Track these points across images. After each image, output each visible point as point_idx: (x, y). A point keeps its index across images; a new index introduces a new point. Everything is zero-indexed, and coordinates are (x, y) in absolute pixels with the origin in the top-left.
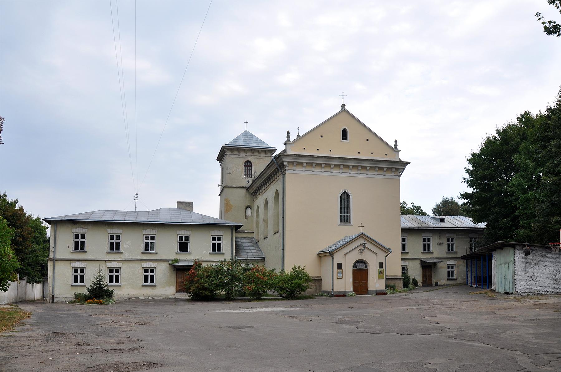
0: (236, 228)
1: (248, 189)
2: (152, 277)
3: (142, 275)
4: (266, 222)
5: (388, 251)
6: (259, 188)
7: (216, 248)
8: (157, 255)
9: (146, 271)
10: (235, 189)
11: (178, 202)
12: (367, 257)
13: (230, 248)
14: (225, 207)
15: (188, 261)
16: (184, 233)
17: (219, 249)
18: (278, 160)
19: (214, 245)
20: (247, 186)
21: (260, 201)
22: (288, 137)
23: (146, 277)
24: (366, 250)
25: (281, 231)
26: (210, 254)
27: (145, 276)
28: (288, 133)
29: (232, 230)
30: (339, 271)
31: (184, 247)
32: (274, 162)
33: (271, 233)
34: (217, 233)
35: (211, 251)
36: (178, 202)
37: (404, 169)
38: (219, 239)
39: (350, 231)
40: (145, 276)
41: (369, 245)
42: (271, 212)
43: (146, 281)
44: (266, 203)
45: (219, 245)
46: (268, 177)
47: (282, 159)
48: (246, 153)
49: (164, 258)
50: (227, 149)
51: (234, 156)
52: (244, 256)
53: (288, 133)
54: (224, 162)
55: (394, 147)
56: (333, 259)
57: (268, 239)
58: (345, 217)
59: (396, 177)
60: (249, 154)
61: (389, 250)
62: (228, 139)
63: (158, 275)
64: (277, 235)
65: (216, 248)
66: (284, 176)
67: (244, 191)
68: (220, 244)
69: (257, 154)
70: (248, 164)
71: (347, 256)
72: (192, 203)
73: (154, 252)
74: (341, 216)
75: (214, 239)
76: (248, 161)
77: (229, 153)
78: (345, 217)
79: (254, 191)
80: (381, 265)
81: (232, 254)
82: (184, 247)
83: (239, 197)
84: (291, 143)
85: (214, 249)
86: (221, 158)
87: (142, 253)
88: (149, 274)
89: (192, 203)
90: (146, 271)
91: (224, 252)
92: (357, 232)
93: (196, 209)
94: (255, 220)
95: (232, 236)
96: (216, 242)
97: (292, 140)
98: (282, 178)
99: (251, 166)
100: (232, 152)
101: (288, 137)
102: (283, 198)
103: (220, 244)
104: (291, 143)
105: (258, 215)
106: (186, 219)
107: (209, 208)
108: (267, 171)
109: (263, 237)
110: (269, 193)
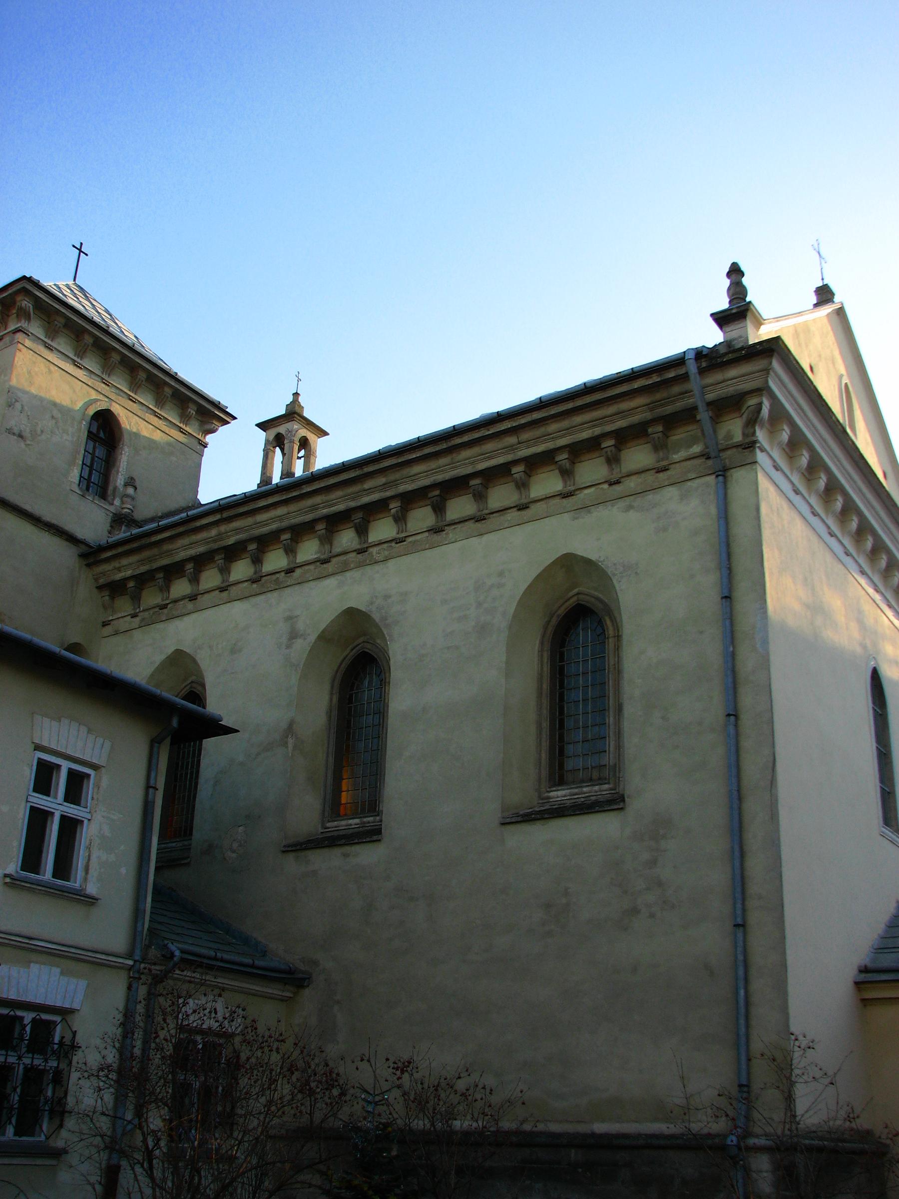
13: (127, 872)
18: (711, 379)
22: (737, 291)
26: (13, 882)
28: (735, 272)
29: (154, 743)
35: (13, 867)
47: (767, 371)
51: (52, 357)
53: (735, 272)
57: (367, 856)
60: (120, 382)
75: (44, 778)
77: (36, 328)
91: (92, 889)
100: (52, 332)
101: (737, 291)
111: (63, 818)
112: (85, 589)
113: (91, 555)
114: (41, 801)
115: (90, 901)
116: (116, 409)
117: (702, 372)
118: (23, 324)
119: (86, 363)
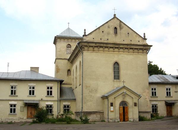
0: (61, 82)
1: (69, 60)
2: (14, 109)
3: (9, 108)
4: (76, 78)
5: (139, 96)
6: (73, 59)
7: (49, 93)
8: (18, 97)
9: (11, 106)
10: (62, 60)
11: (31, 67)
12: (128, 100)
14: (57, 70)
15: (34, 101)
16: (32, 84)
17: (51, 94)
19: (48, 92)
20: (68, 58)
21: (74, 67)
22: (85, 33)
23: (11, 109)
24: (126, 95)
25: (81, 84)
26: (46, 96)
27: (11, 109)
28: (85, 30)
29: (58, 83)
30: (111, 107)
31: (32, 93)
32: (78, 47)
33: (78, 85)
34: (50, 85)
36: (31, 67)
37: (150, 49)
38: (51, 88)
39: (118, 84)
40: (11, 109)
41: (128, 93)
42: (78, 73)
43: (11, 112)
44: (76, 68)
45: (51, 92)
46: (77, 54)
48: (68, 40)
49: (21, 99)
50: (58, 38)
51: (62, 42)
52: (65, 98)
53: (85, 30)
54: (56, 45)
55: (143, 37)
56: (108, 100)
58: (117, 76)
59: (146, 54)
60: (70, 40)
61: (139, 95)
62: (58, 33)
63: (18, 108)
64: (81, 86)
65: (49, 93)
66: (83, 53)
67: (66, 61)
68: (52, 91)
69: (74, 41)
70: (69, 46)
71: (116, 98)
72: (39, 68)
73: (16, 95)
74: (114, 76)
75: (48, 88)
76: (69, 45)
77: (59, 40)
78: (117, 76)
79: (72, 60)
80: (135, 105)
81: (58, 97)
82: (32, 93)
83: (64, 64)
84: (86, 36)
85: (48, 94)
86: (55, 43)
87: (10, 96)
88: (13, 108)
89: (39, 68)
90: (11, 106)
92: (121, 85)
93: (41, 71)
94: (72, 77)
95: (58, 87)
96: (50, 90)
97: (87, 34)
98: (82, 55)
99: (71, 47)
101: (85, 33)
102: (82, 66)
103: (52, 91)
104: (86, 36)
105: (73, 75)
106: (34, 77)
107: (48, 70)
108: (75, 51)
109: (75, 87)
110: (77, 63)
111: (50, 91)
112: (69, 63)
113: (69, 60)
114: (48, 90)
115: (53, 97)
116: (70, 44)
117: (79, 45)
118: (57, 40)
119: (65, 41)
